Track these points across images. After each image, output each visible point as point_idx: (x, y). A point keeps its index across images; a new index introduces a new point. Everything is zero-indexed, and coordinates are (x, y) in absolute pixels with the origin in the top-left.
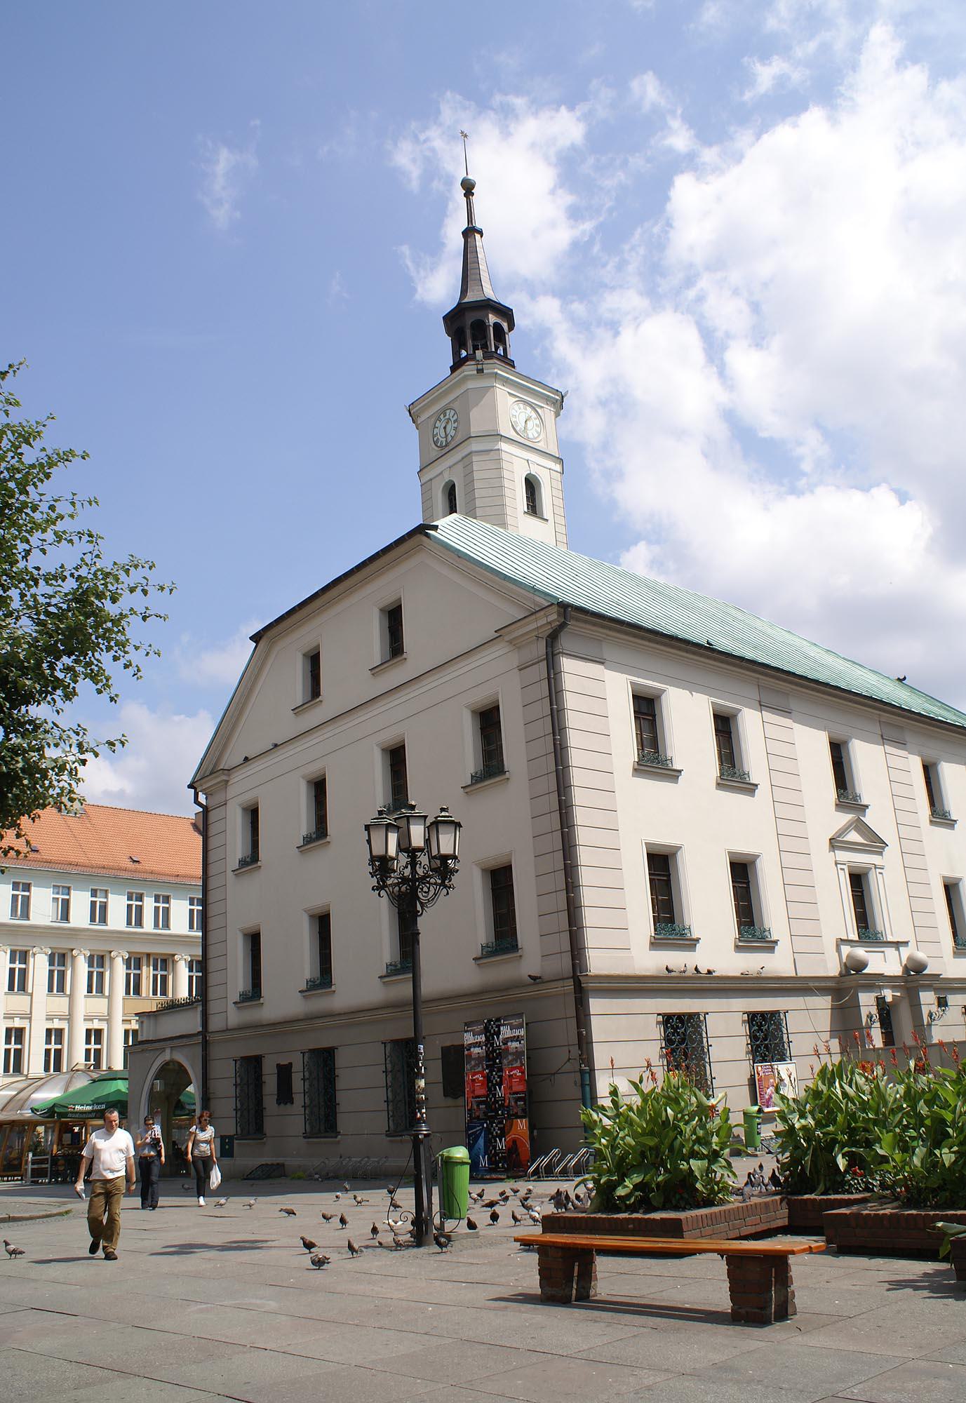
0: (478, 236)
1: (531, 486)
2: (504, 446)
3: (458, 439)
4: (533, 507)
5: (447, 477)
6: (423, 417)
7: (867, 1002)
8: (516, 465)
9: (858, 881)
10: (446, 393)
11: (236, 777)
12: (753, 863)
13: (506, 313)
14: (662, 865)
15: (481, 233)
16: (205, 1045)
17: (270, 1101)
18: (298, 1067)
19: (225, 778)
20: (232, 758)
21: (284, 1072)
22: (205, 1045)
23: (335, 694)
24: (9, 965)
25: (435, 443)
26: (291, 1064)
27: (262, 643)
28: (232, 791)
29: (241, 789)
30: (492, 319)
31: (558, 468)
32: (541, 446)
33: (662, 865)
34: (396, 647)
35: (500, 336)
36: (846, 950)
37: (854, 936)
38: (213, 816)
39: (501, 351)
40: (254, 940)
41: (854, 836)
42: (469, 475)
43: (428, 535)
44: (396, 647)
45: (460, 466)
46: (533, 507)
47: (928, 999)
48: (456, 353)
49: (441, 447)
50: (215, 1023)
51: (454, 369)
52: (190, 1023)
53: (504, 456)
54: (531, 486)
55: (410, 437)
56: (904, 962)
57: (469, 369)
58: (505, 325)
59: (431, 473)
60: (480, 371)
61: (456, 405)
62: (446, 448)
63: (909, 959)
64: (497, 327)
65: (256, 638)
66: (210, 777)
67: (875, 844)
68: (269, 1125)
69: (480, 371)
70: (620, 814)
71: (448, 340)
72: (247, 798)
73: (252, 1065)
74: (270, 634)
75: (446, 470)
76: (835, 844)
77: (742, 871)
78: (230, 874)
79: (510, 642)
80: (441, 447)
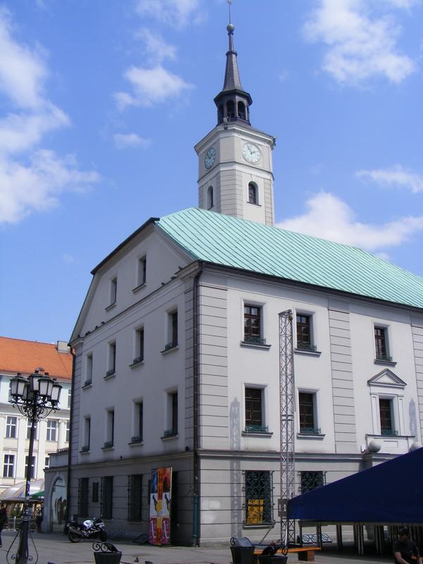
0: (234, 56)
1: (253, 187)
2: (237, 167)
3: (215, 165)
4: (254, 199)
5: (209, 184)
6: (201, 152)
8: (245, 176)
12: (315, 393)
15: (236, 54)
16: (70, 471)
17: (90, 500)
19: (81, 341)
21: (96, 485)
22: (70, 471)
24: (7, 424)
25: (205, 166)
27: (96, 275)
28: (85, 348)
30: (238, 99)
31: (269, 177)
32: (260, 166)
33: (255, 396)
36: (370, 440)
37: (378, 431)
38: (77, 360)
41: (386, 379)
42: (218, 183)
43: (155, 223)
46: (254, 199)
50: (74, 462)
52: (64, 461)
54: (253, 187)
56: (410, 446)
58: (245, 102)
59: (203, 183)
60: (226, 128)
61: (214, 147)
62: (210, 169)
64: (241, 104)
65: (94, 272)
66: (76, 341)
67: (400, 383)
69: (226, 128)
71: (216, 109)
73: (85, 481)
74: (99, 270)
78: (82, 390)
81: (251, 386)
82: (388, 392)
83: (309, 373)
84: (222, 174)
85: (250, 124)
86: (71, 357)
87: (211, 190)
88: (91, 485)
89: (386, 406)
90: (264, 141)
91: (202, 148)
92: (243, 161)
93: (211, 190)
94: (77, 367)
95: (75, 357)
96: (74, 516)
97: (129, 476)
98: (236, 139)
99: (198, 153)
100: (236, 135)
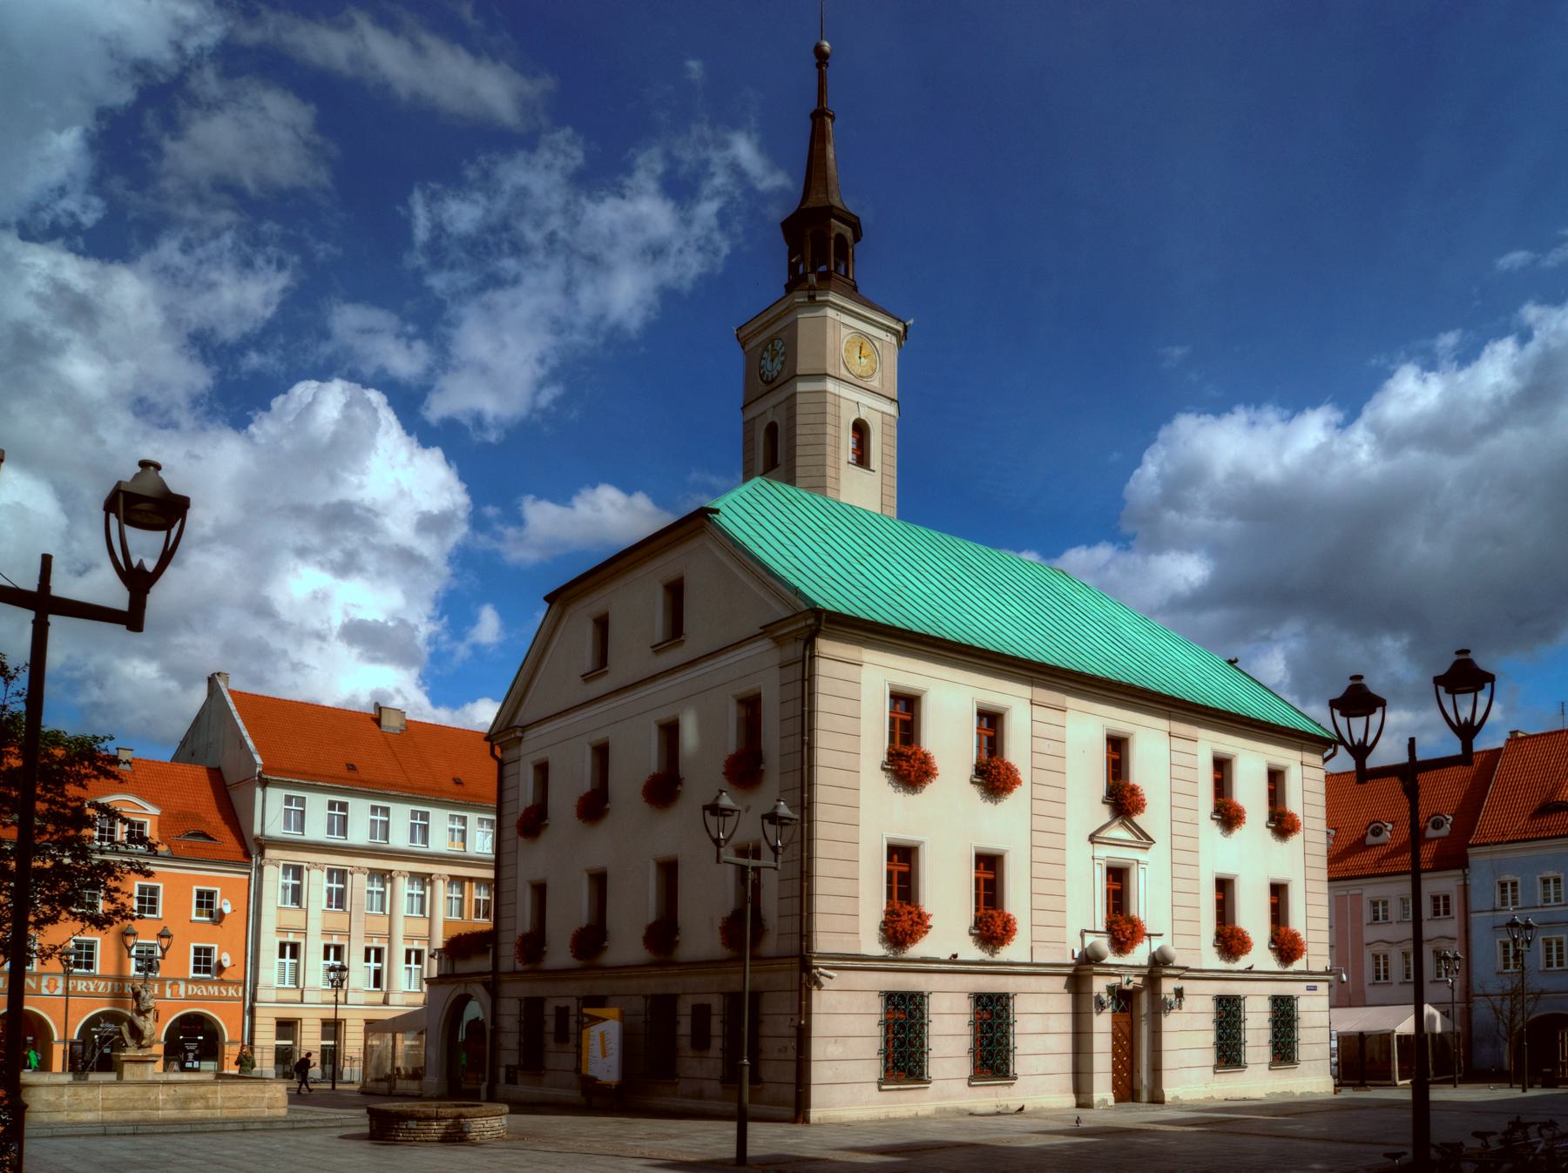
2: (830, 386)
6: (753, 344)
7: (1100, 985)
9: (1118, 876)
10: (779, 317)
11: (530, 735)
13: (855, 224)
14: (903, 859)
18: (573, 1011)
20: (524, 717)
23: (623, 667)
26: (567, 1008)
29: (533, 747)
32: (875, 383)
34: (676, 630)
35: (843, 252)
38: (509, 770)
39: (842, 270)
40: (540, 890)
44: (676, 630)
45: (784, 406)
47: (1168, 987)
48: (792, 268)
49: (767, 383)
51: (790, 288)
53: (830, 398)
55: (735, 359)
56: (1154, 949)
57: (800, 297)
62: (772, 384)
63: (1160, 949)
65: (550, 599)
67: (1145, 839)
68: (551, 1061)
70: (858, 811)
72: (539, 756)
75: (767, 409)
76: (1093, 839)
77: (989, 866)
79: (775, 639)
80: (767, 383)
81: (897, 843)
82: (1121, 855)
83: (1002, 825)
84: (799, 399)
85: (855, 288)
86: (495, 763)
87: (772, 429)
88: (549, 1009)
89: (1118, 876)
90: (888, 329)
91: (755, 334)
92: (844, 373)
93: (772, 429)
94: (509, 783)
95: (501, 765)
96: (508, 1067)
97: (646, 997)
98: (829, 322)
99: (743, 343)
100: (830, 313)
